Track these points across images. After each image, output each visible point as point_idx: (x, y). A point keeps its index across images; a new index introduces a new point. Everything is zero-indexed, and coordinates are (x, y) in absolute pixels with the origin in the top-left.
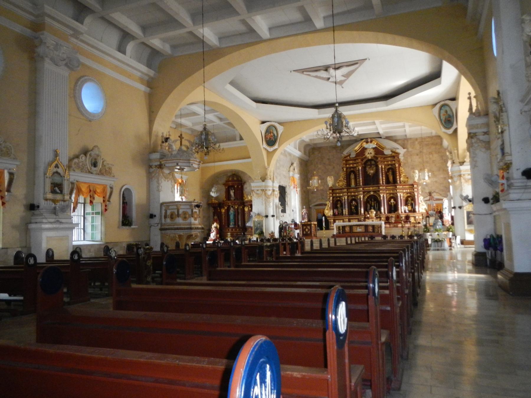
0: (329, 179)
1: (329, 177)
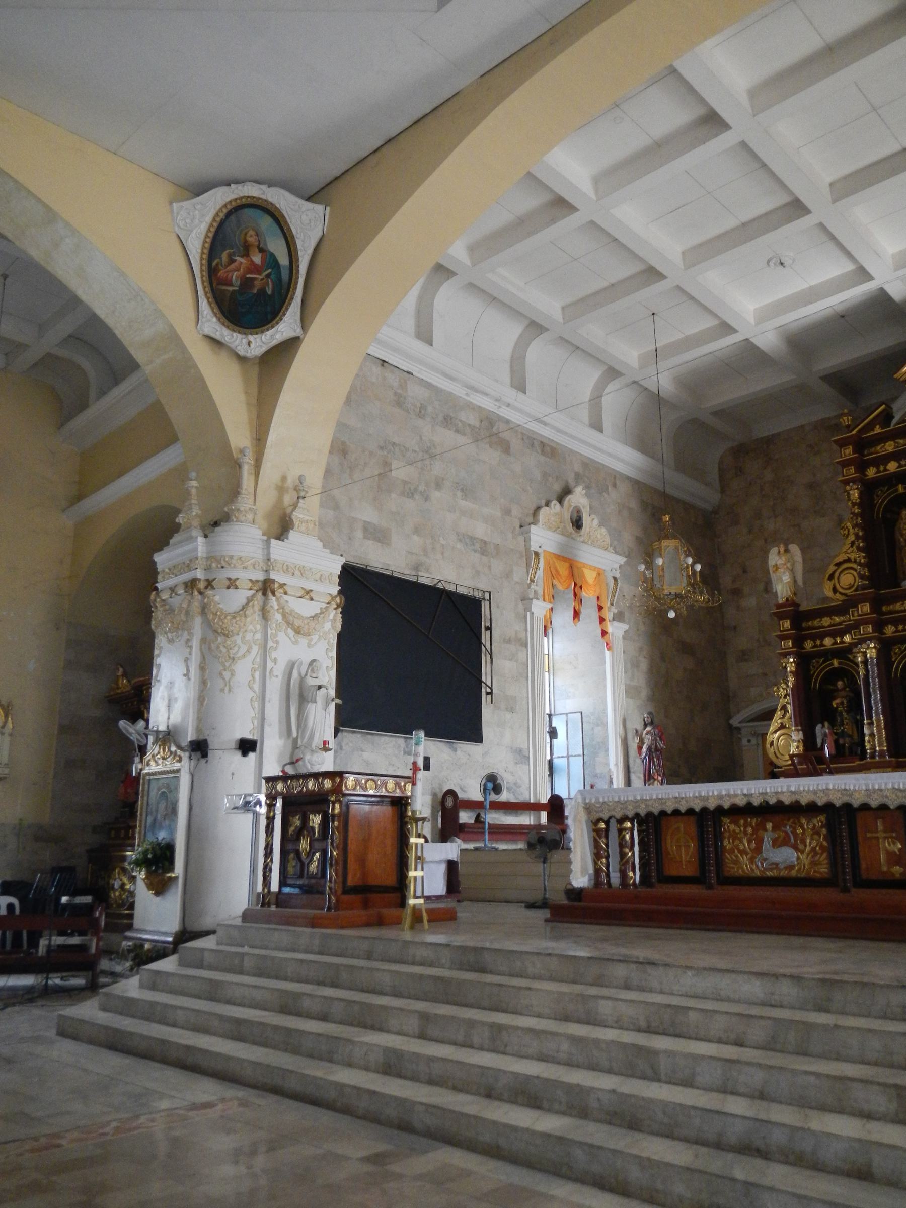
0: (775, 558)
1: (774, 550)
